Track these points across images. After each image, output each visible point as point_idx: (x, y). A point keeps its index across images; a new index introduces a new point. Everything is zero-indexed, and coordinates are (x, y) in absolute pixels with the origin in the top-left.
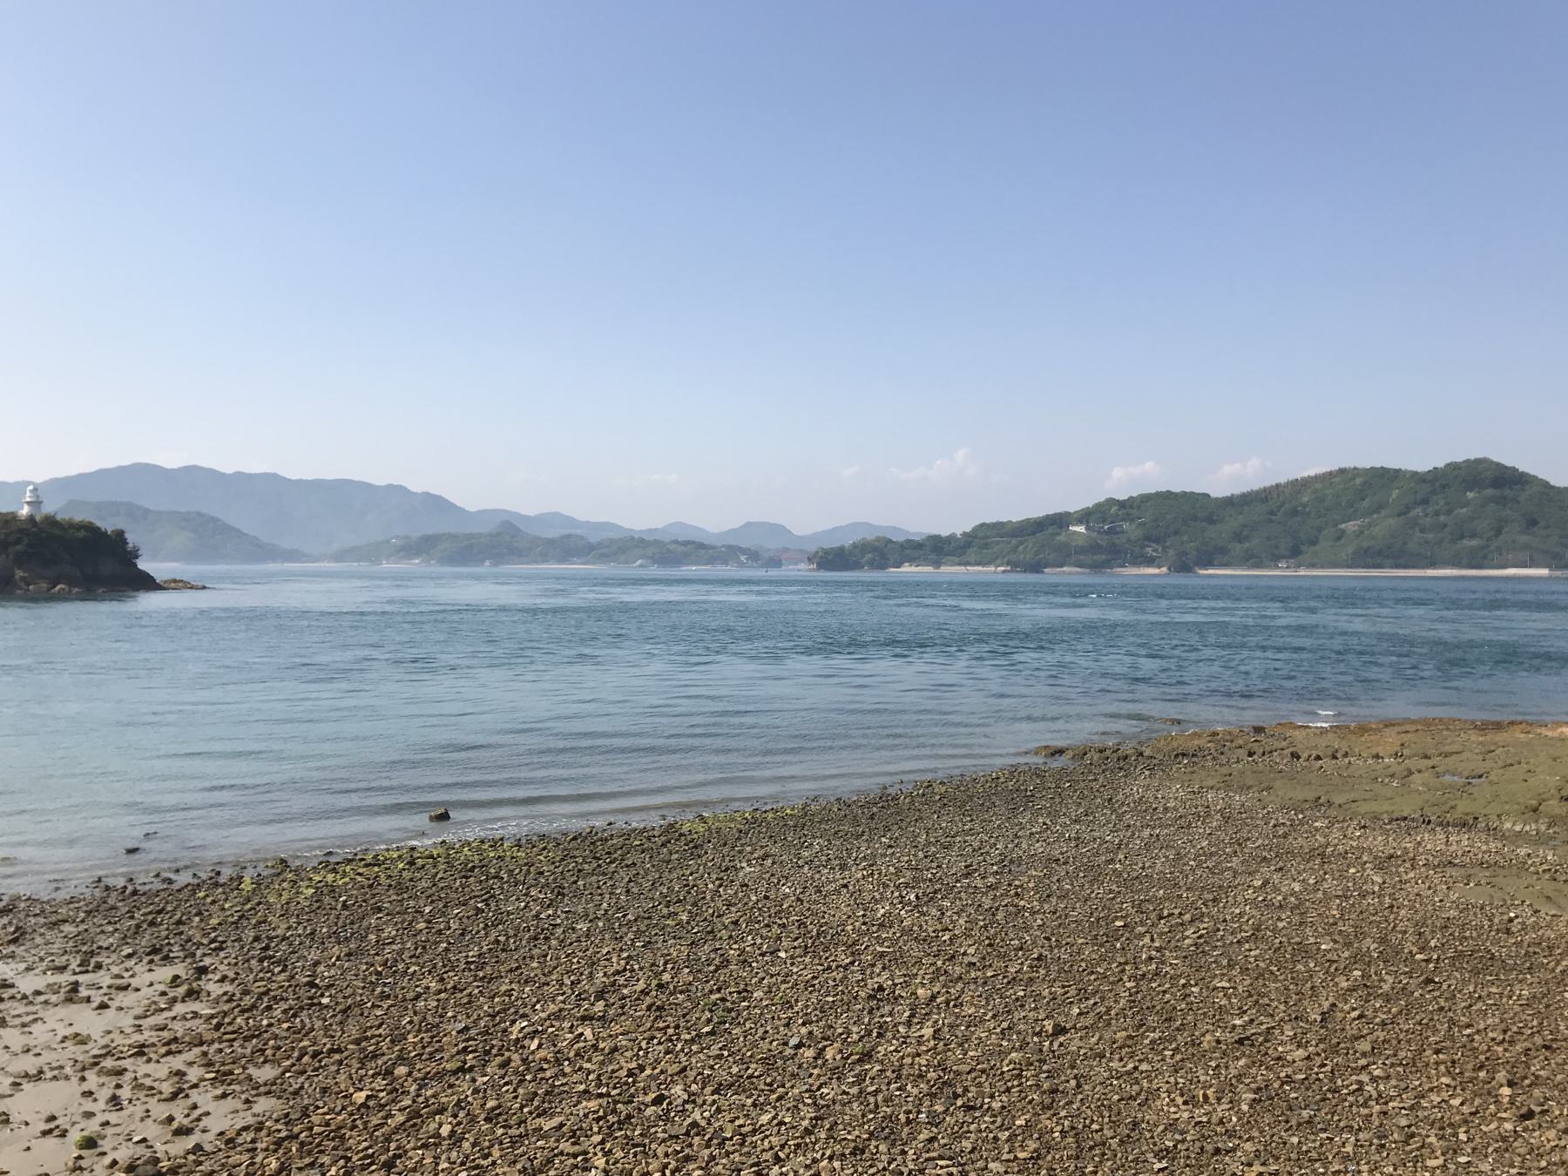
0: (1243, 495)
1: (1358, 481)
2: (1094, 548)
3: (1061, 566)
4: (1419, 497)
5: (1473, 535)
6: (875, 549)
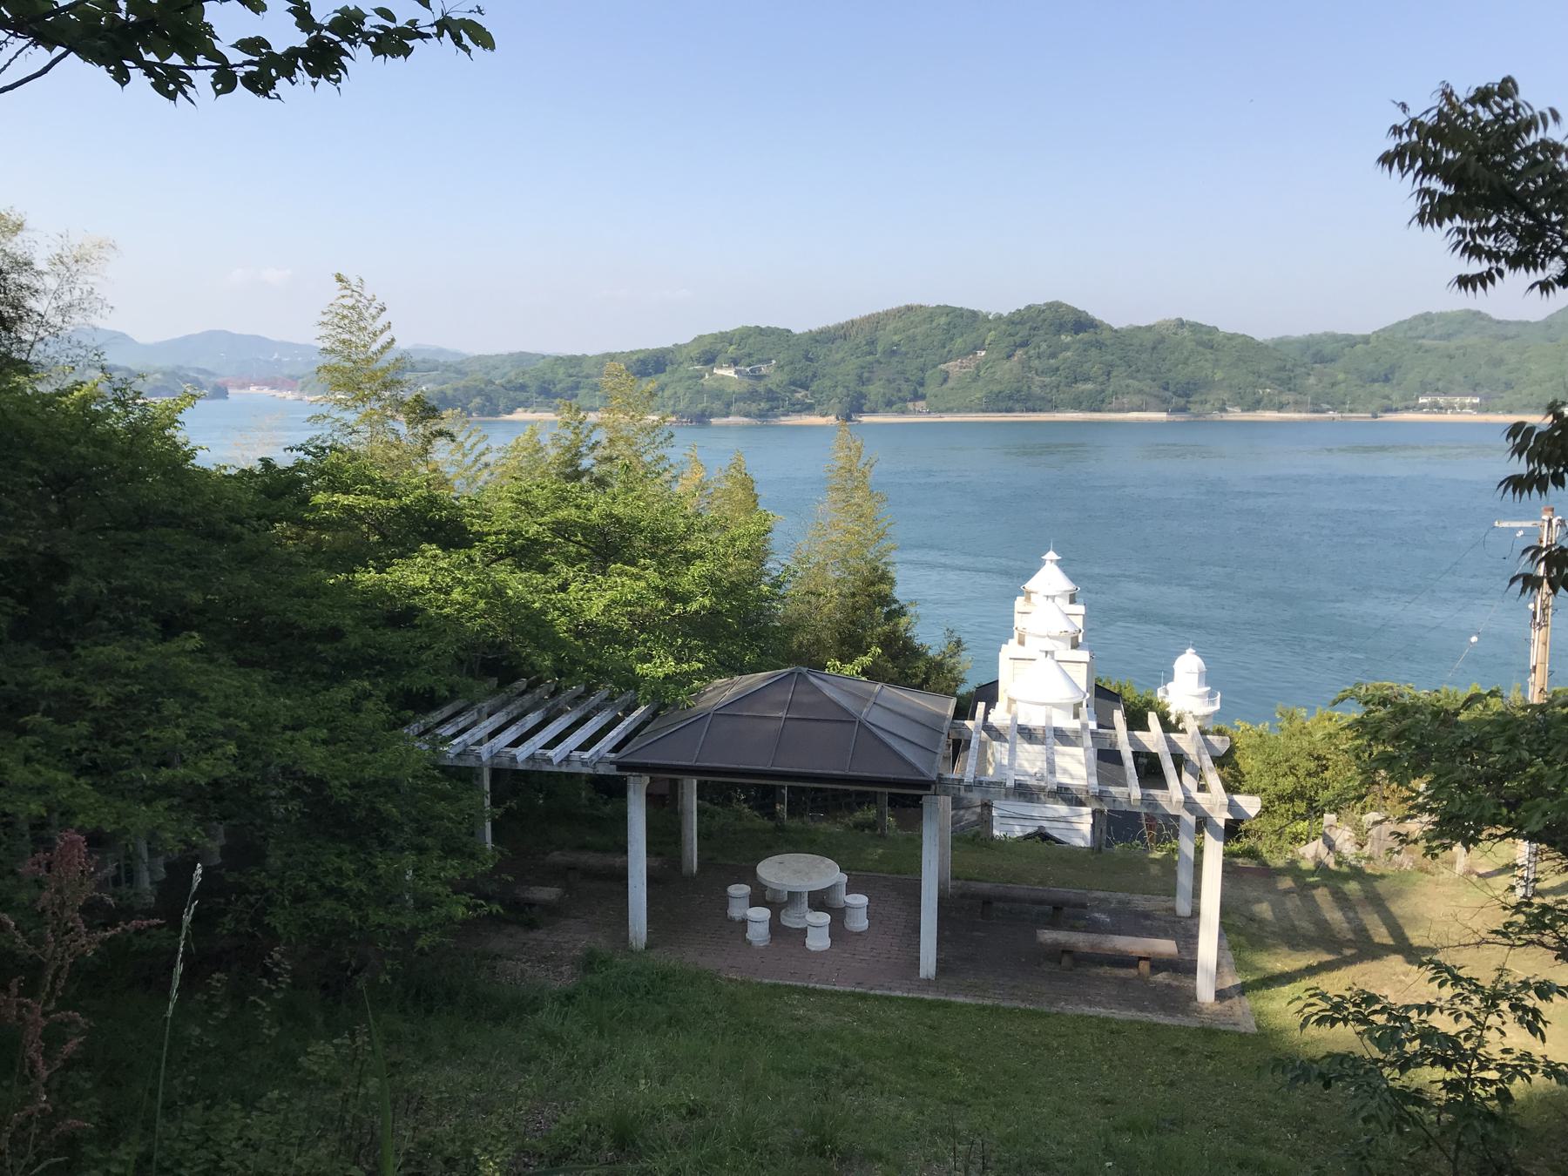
0: (821, 332)
1: (943, 320)
2: (753, 396)
3: (727, 415)
4: (1018, 339)
5: (1087, 380)
6: (480, 393)
